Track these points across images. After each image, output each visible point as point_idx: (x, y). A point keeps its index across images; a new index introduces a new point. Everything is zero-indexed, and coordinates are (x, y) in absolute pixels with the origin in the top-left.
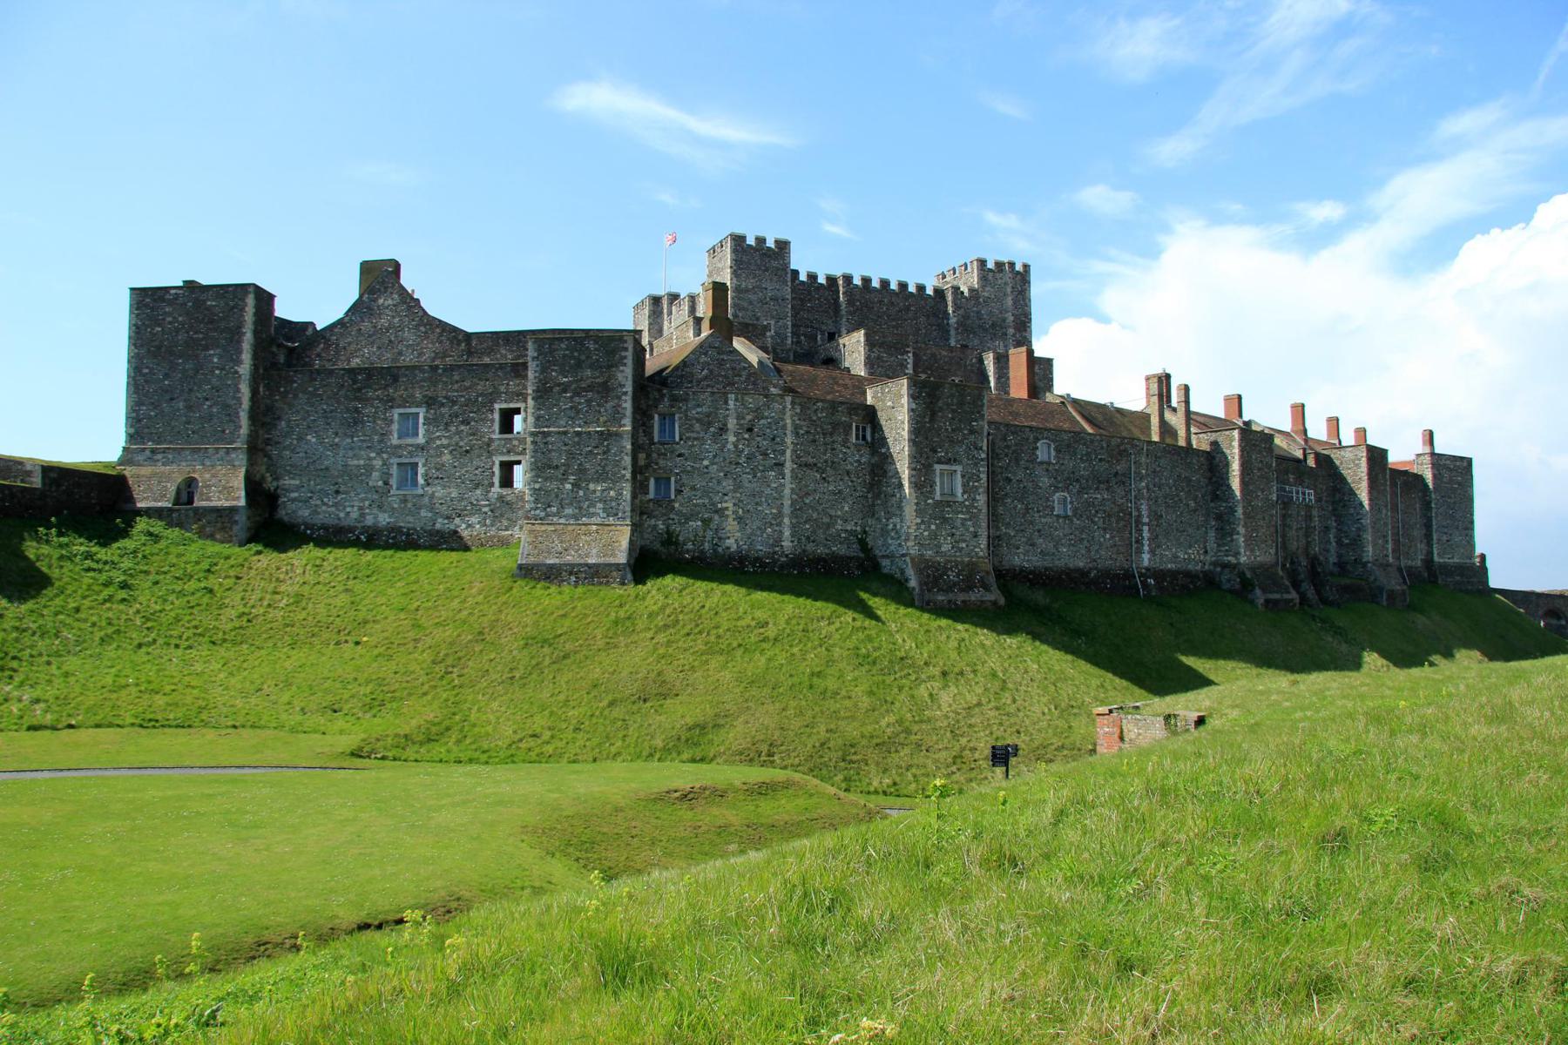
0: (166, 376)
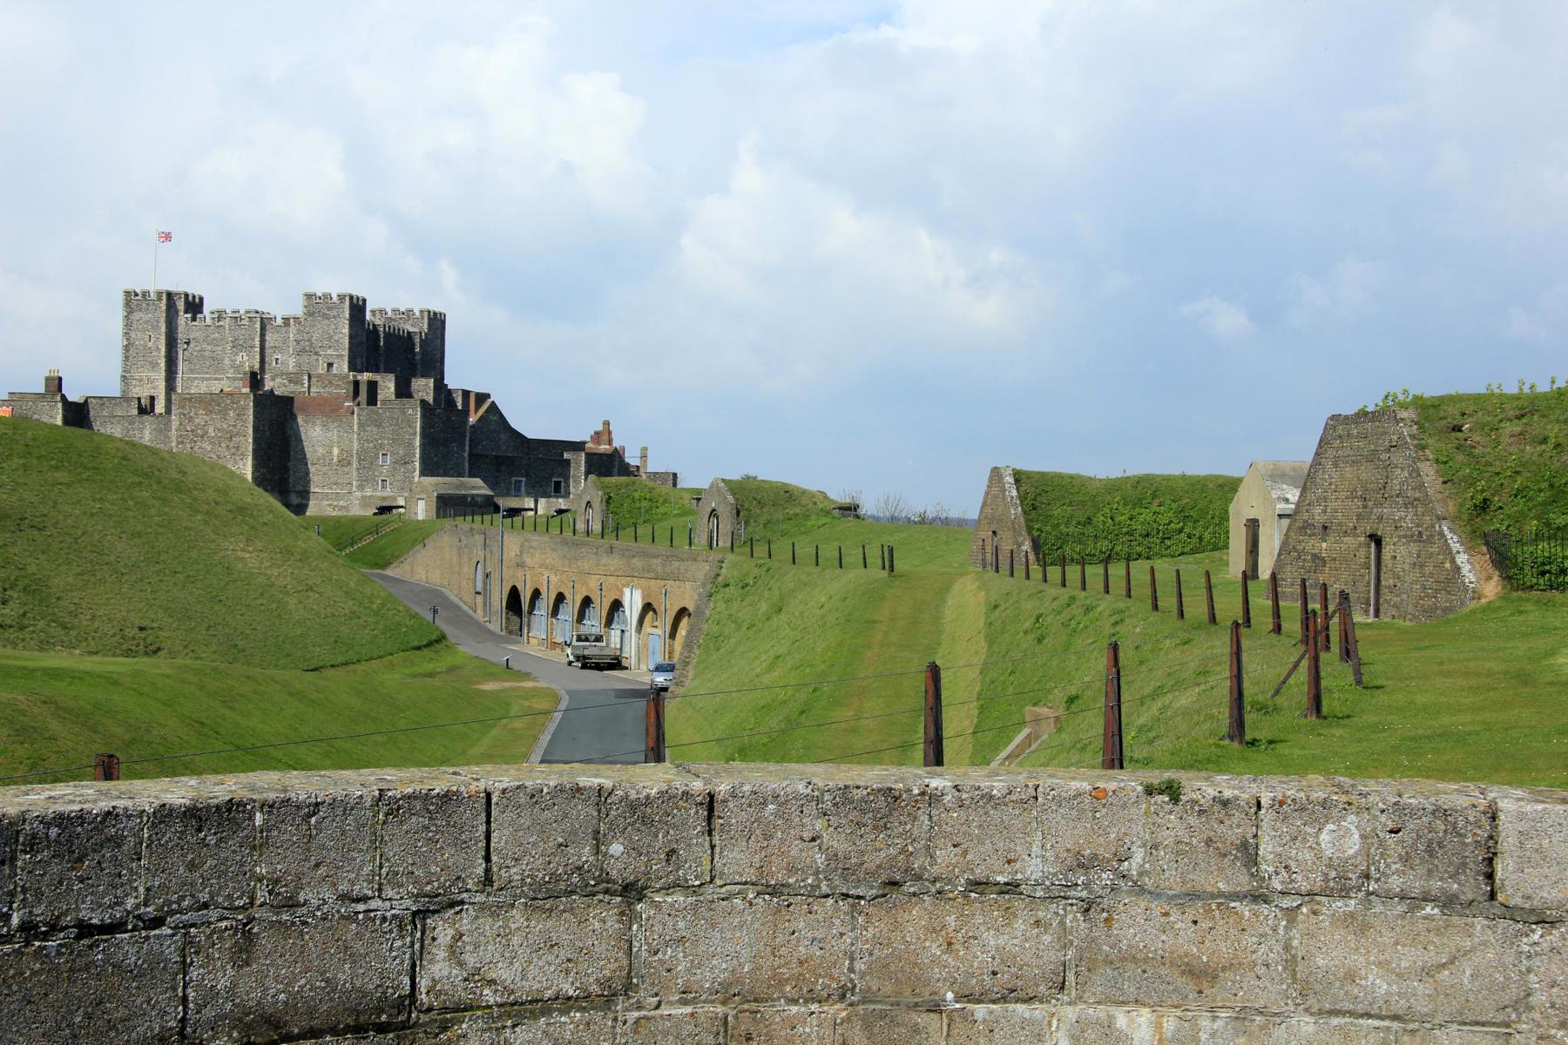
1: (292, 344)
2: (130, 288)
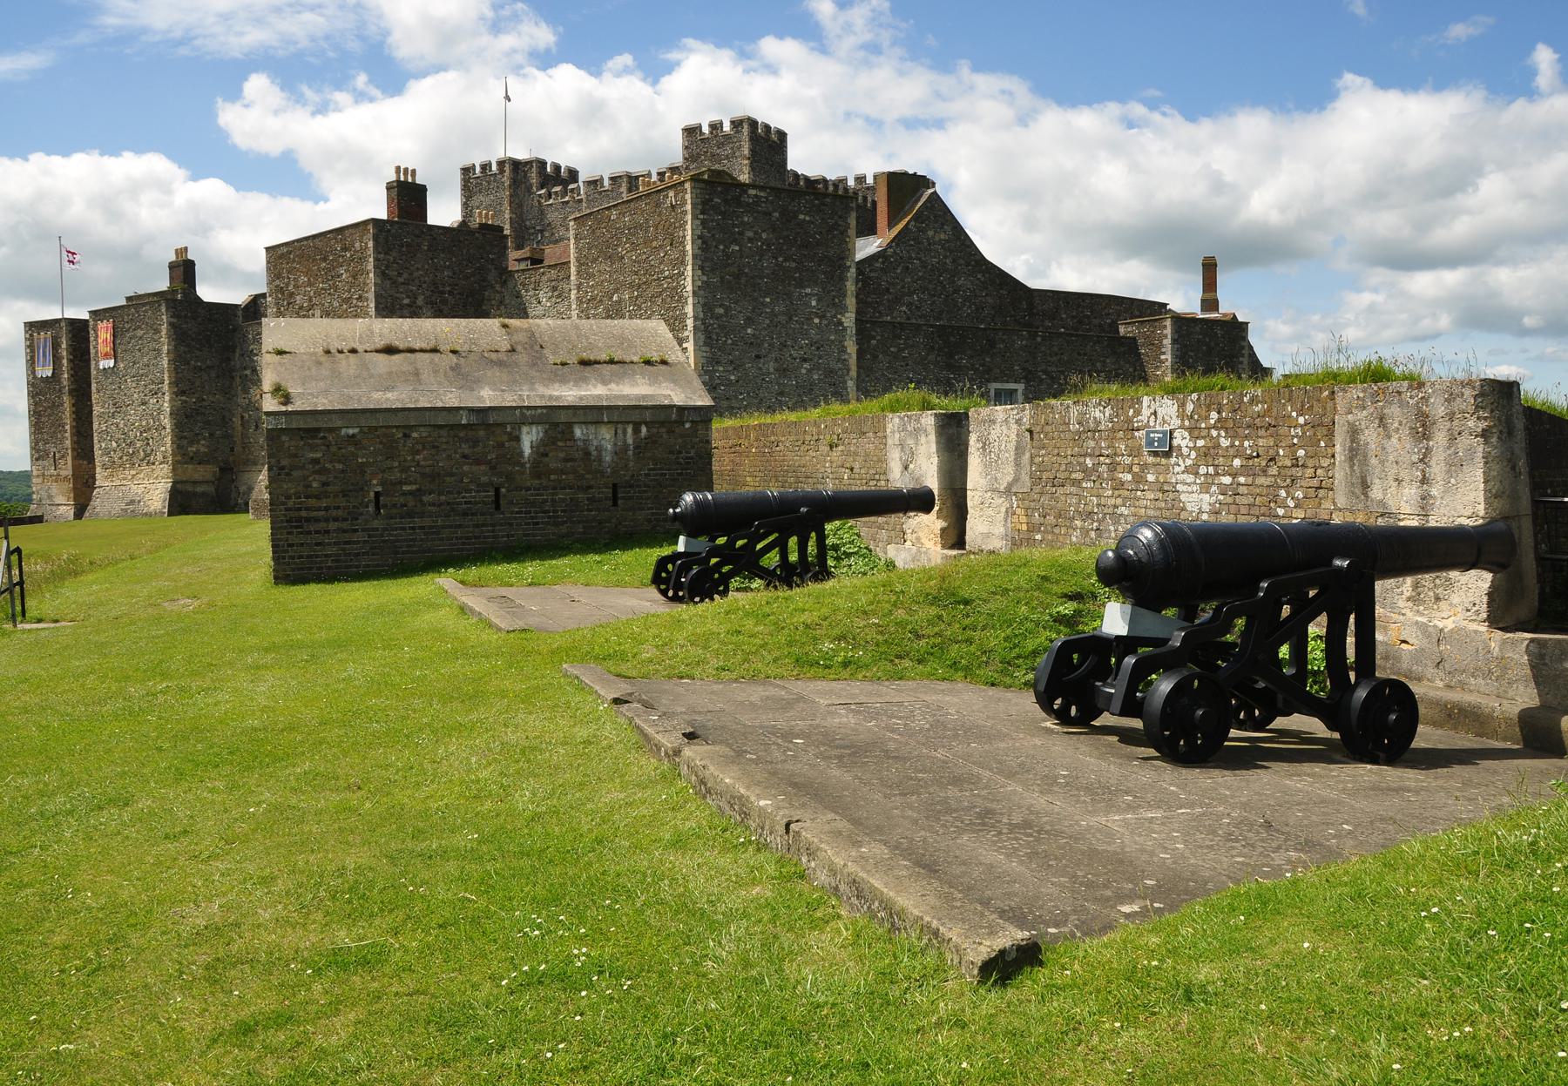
0: (750, 321)
2: (467, 163)
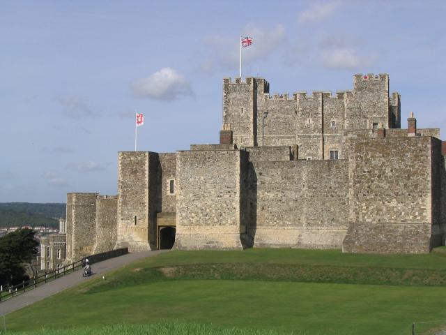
1: (347, 110)
